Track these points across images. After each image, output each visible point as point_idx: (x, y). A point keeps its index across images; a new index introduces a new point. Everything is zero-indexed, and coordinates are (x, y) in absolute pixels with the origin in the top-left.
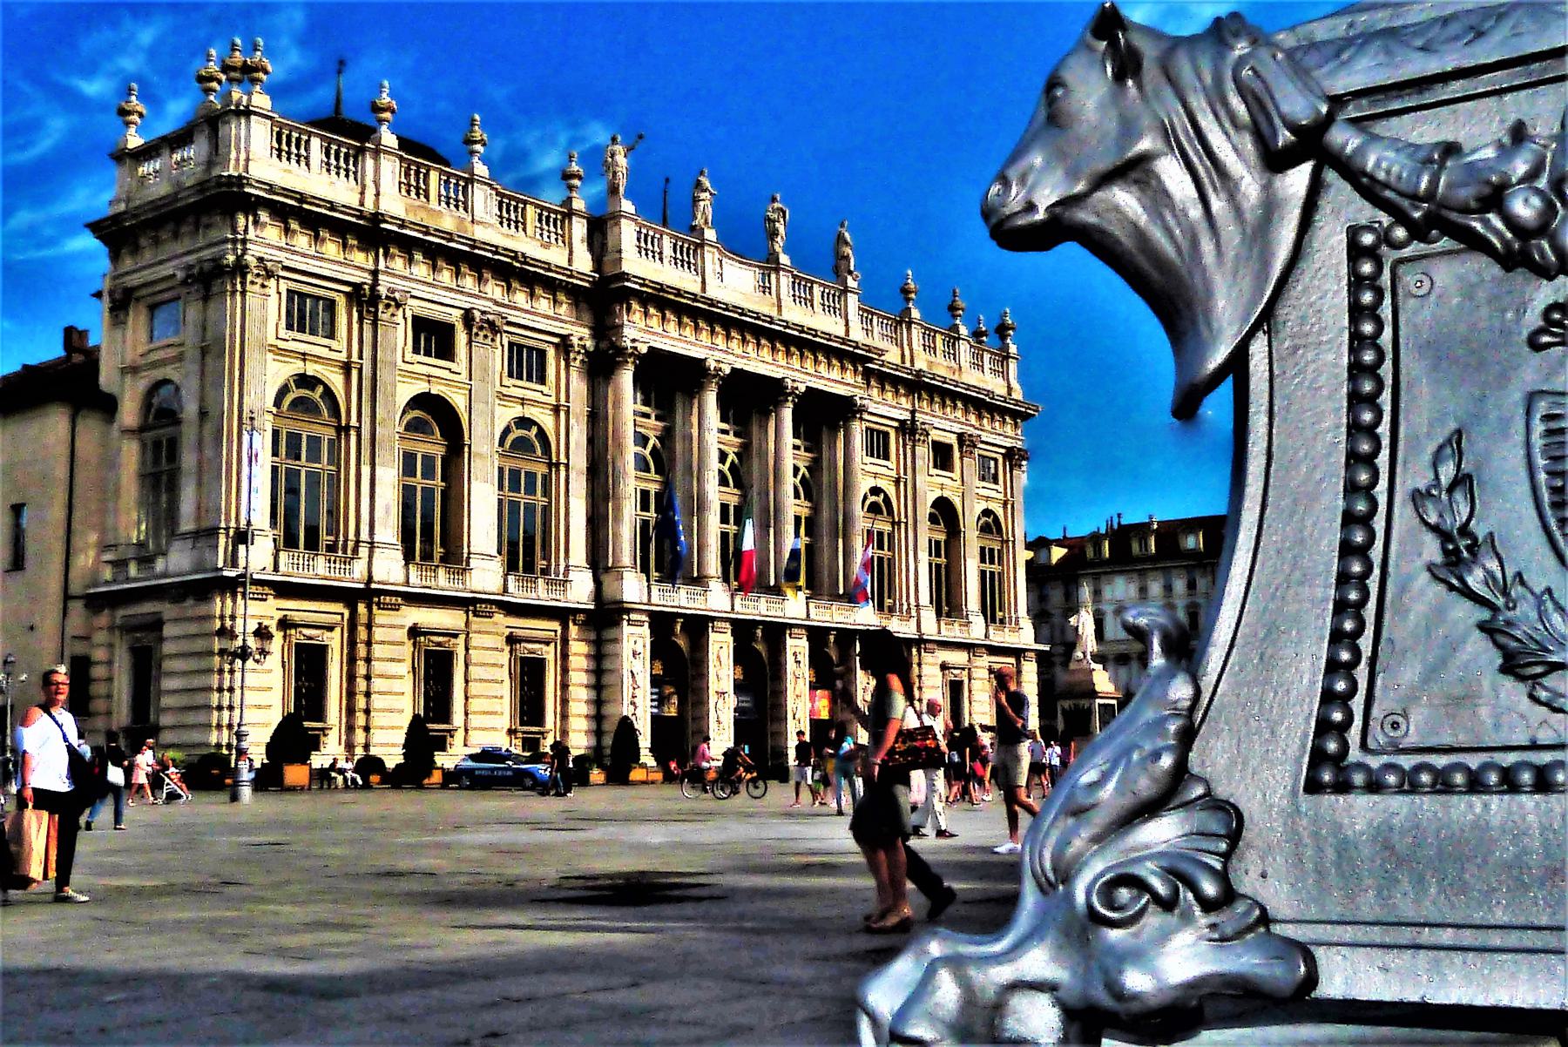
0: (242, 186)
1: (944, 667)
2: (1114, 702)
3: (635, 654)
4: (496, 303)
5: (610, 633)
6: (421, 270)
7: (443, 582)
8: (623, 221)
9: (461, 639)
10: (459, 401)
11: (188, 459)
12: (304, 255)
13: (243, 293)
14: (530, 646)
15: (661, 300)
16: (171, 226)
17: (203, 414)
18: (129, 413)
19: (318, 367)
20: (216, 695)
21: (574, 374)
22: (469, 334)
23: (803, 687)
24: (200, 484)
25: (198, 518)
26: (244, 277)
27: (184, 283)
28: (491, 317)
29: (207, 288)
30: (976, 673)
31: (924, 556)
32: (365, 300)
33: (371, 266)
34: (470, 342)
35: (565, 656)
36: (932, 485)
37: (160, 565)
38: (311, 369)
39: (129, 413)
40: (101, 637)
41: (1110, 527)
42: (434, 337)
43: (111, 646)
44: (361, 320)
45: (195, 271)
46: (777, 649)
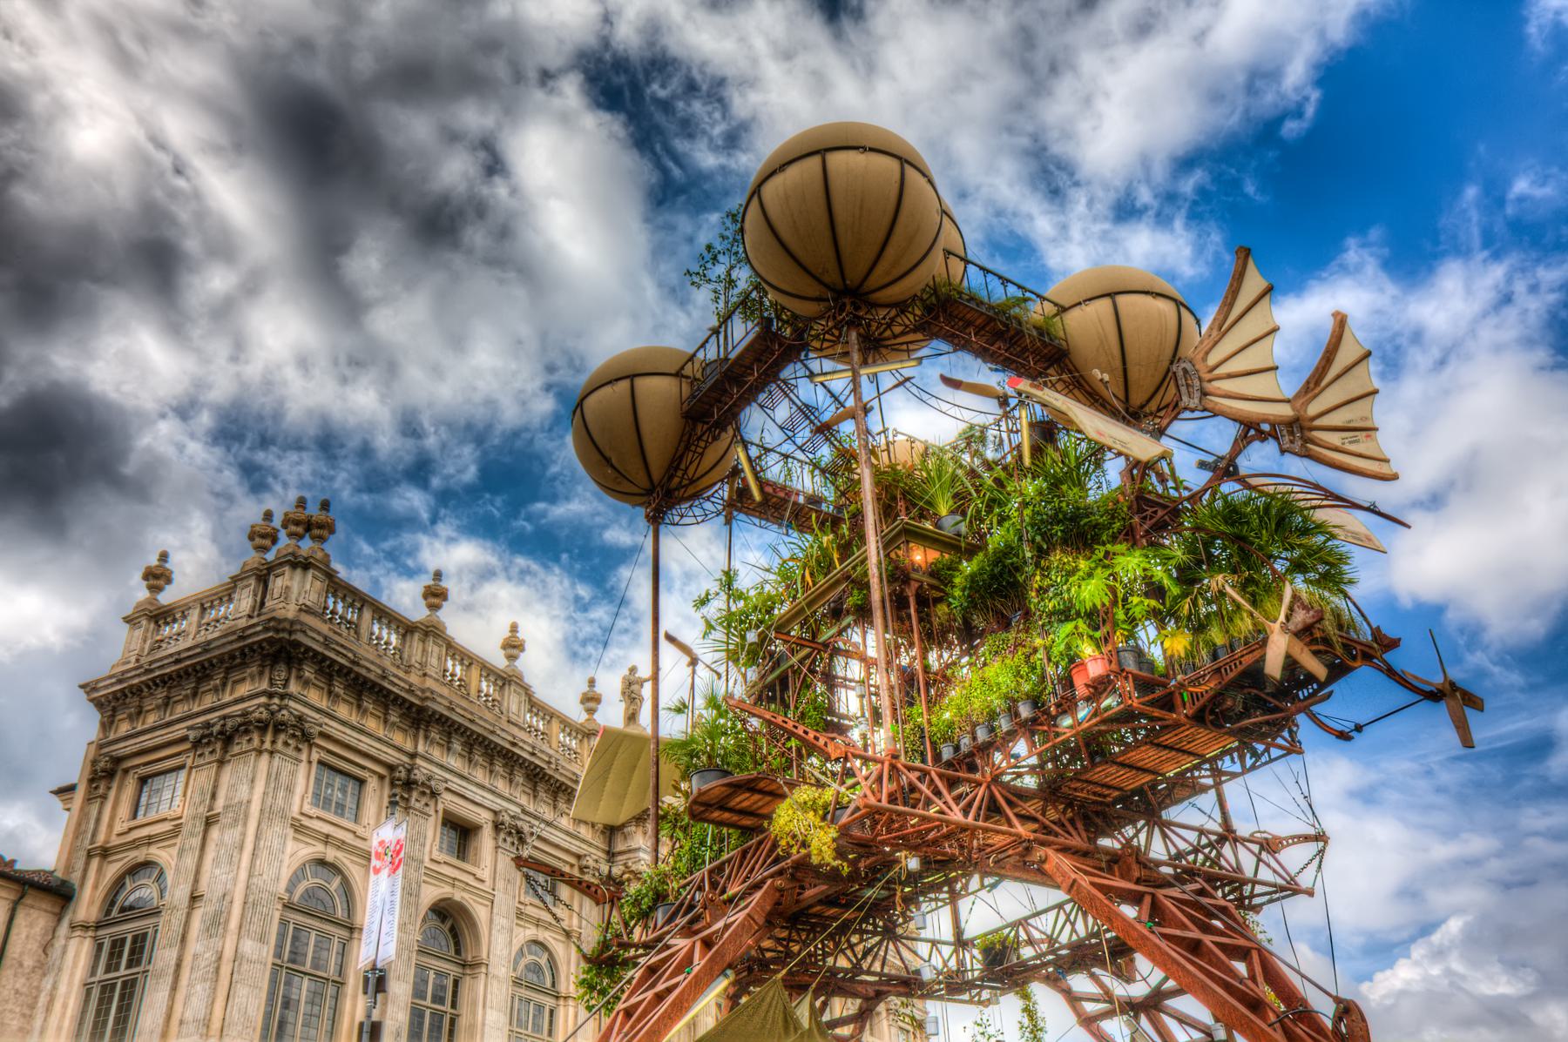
4: (524, 811)
6: (455, 762)
10: (480, 913)
12: (343, 723)
13: (271, 753)
17: (194, 898)
18: (87, 906)
19: (340, 854)
24: (174, 988)
26: (277, 731)
27: (197, 744)
28: (519, 823)
29: (225, 750)
33: (409, 747)
34: (497, 847)
38: (331, 854)
39: (87, 906)
45: (216, 729)
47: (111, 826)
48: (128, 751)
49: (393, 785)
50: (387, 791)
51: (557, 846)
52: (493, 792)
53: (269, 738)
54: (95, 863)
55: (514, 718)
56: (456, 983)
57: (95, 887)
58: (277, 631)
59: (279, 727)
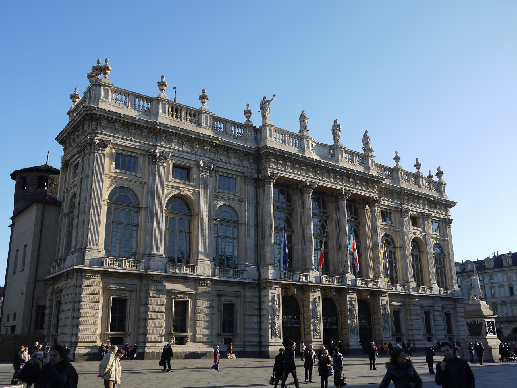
0: (92, 110)
2: (493, 320)
13: (94, 153)
14: (228, 298)
15: (283, 157)
16: (76, 133)
18: (66, 208)
19: (130, 184)
20: (70, 320)
22: (199, 171)
26: (95, 146)
30: (437, 309)
35: (245, 302)
36: (411, 232)
40: (48, 297)
41: (494, 257)
43: (51, 300)
47: (69, 183)
48: (68, 159)
49: (149, 158)
50: (147, 160)
51: (232, 170)
52: (195, 155)
57: (67, 202)
58: (87, 111)
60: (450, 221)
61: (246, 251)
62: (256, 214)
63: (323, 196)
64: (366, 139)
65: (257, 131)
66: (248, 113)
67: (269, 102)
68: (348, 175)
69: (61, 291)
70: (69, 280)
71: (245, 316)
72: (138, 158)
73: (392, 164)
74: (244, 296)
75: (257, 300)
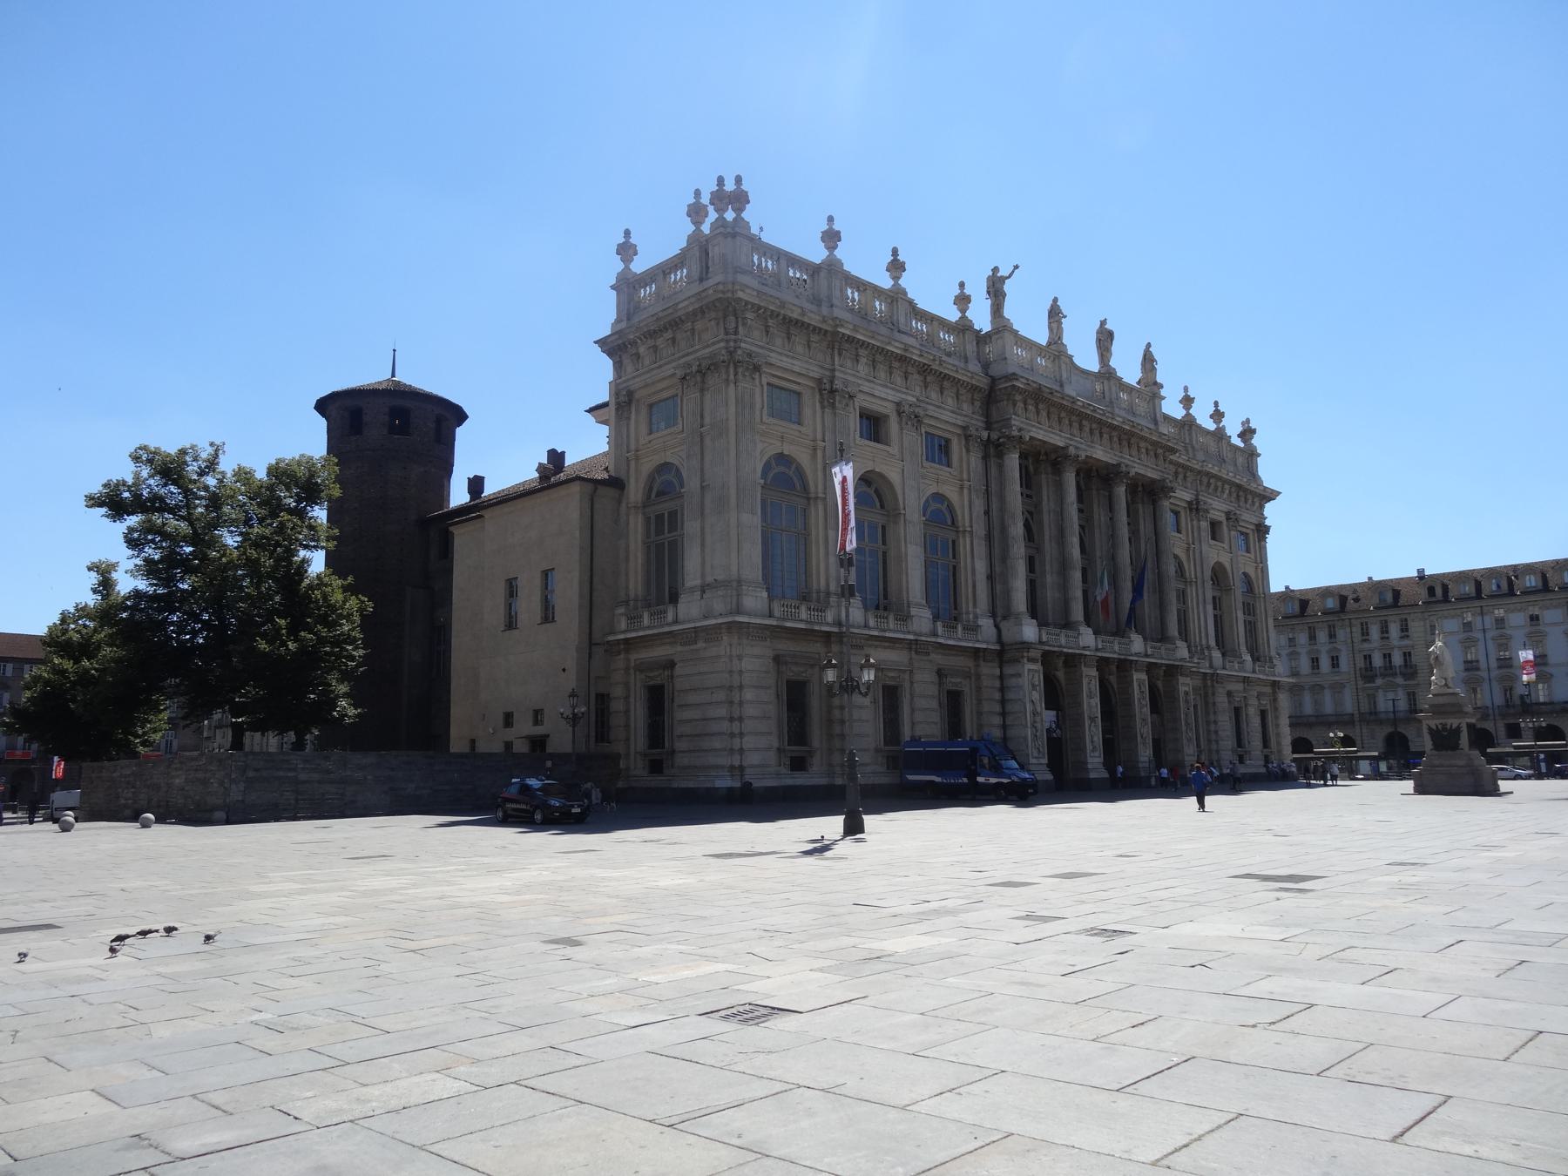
1: (1229, 694)
3: (1034, 687)
5: (1009, 670)
6: (863, 368)
7: (893, 630)
8: (1007, 334)
9: (907, 676)
10: (894, 476)
11: (691, 526)
15: (1039, 398)
16: (669, 335)
17: (702, 488)
18: (635, 492)
21: (973, 460)
22: (900, 423)
23: (1147, 710)
25: (703, 576)
31: (1210, 608)
32: (829, 393)
35: (979, 689)
36: (1215, 553)
37: (670, 617)
39: (635, 492)
42: (873, 426)
44: (823, 407)
45: (694, 368)
46: (1126, 682)
53: (732, 370)
54: (633, 464)
55: (902, 327)
56: (883, 528)
59: (737, 364)
60: (1267, 530)
61: (974, 586)
62: (987, 513)
63: (1096, 478)
64: (1148, 361)
65: (981, 339)
66: (963, 300)
67: (1003, 279)
68: (1125, 437)
69: (671, 665)
70: (701, 644)
71: (980, 714)
72: (799, 394)
73: (1178, 413)
74: (978, 677)
75: (997, 684)
